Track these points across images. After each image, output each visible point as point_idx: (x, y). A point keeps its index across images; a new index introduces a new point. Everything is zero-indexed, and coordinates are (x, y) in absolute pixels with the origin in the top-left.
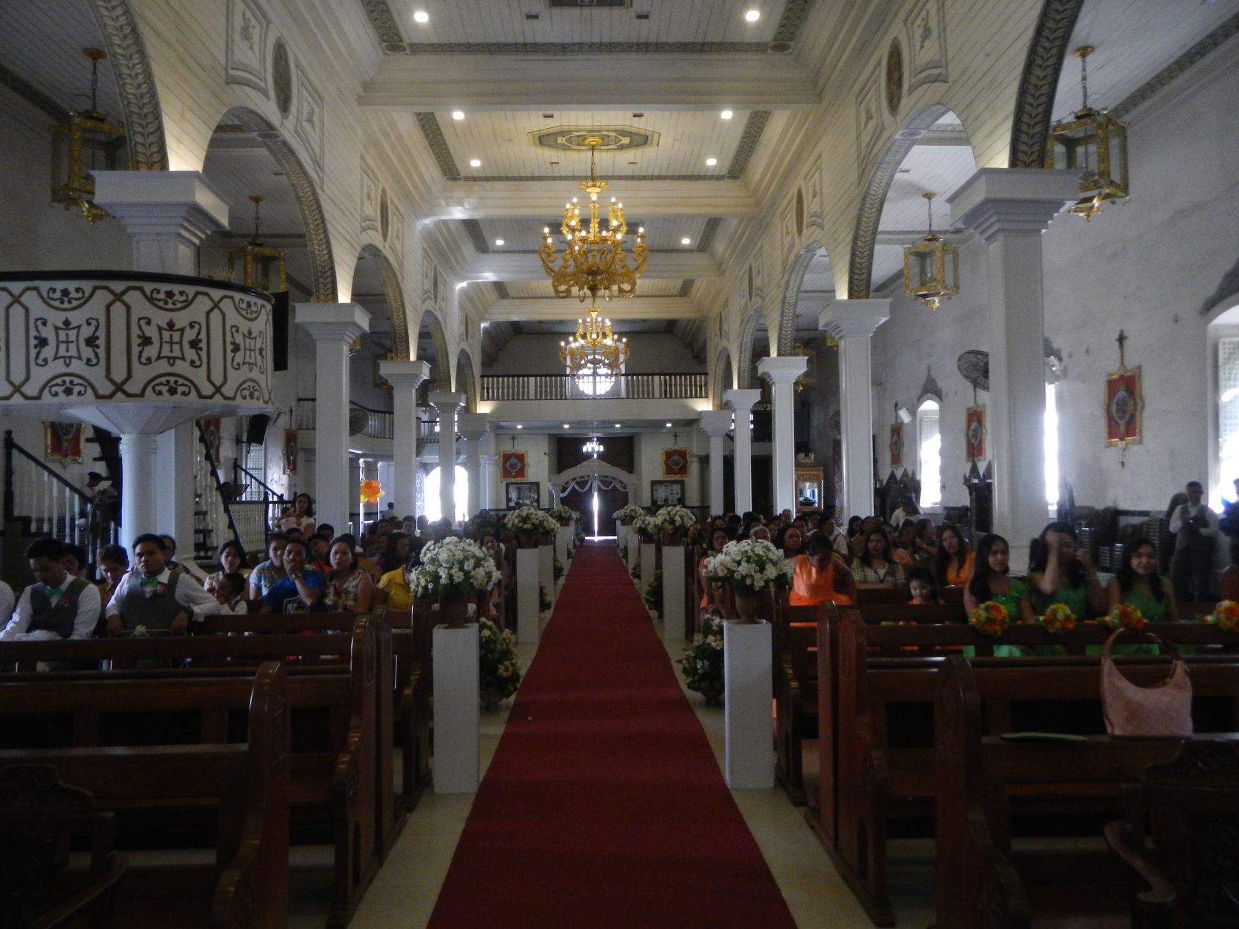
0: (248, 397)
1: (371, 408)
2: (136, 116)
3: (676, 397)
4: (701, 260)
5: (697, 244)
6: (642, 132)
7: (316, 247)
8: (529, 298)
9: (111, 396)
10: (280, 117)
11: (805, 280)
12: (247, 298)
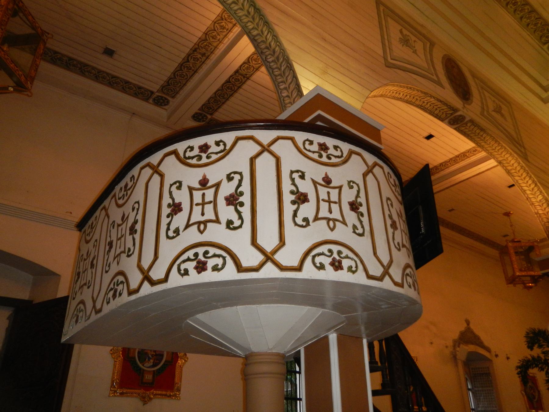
0: (329, 269)
10: (462, 103)
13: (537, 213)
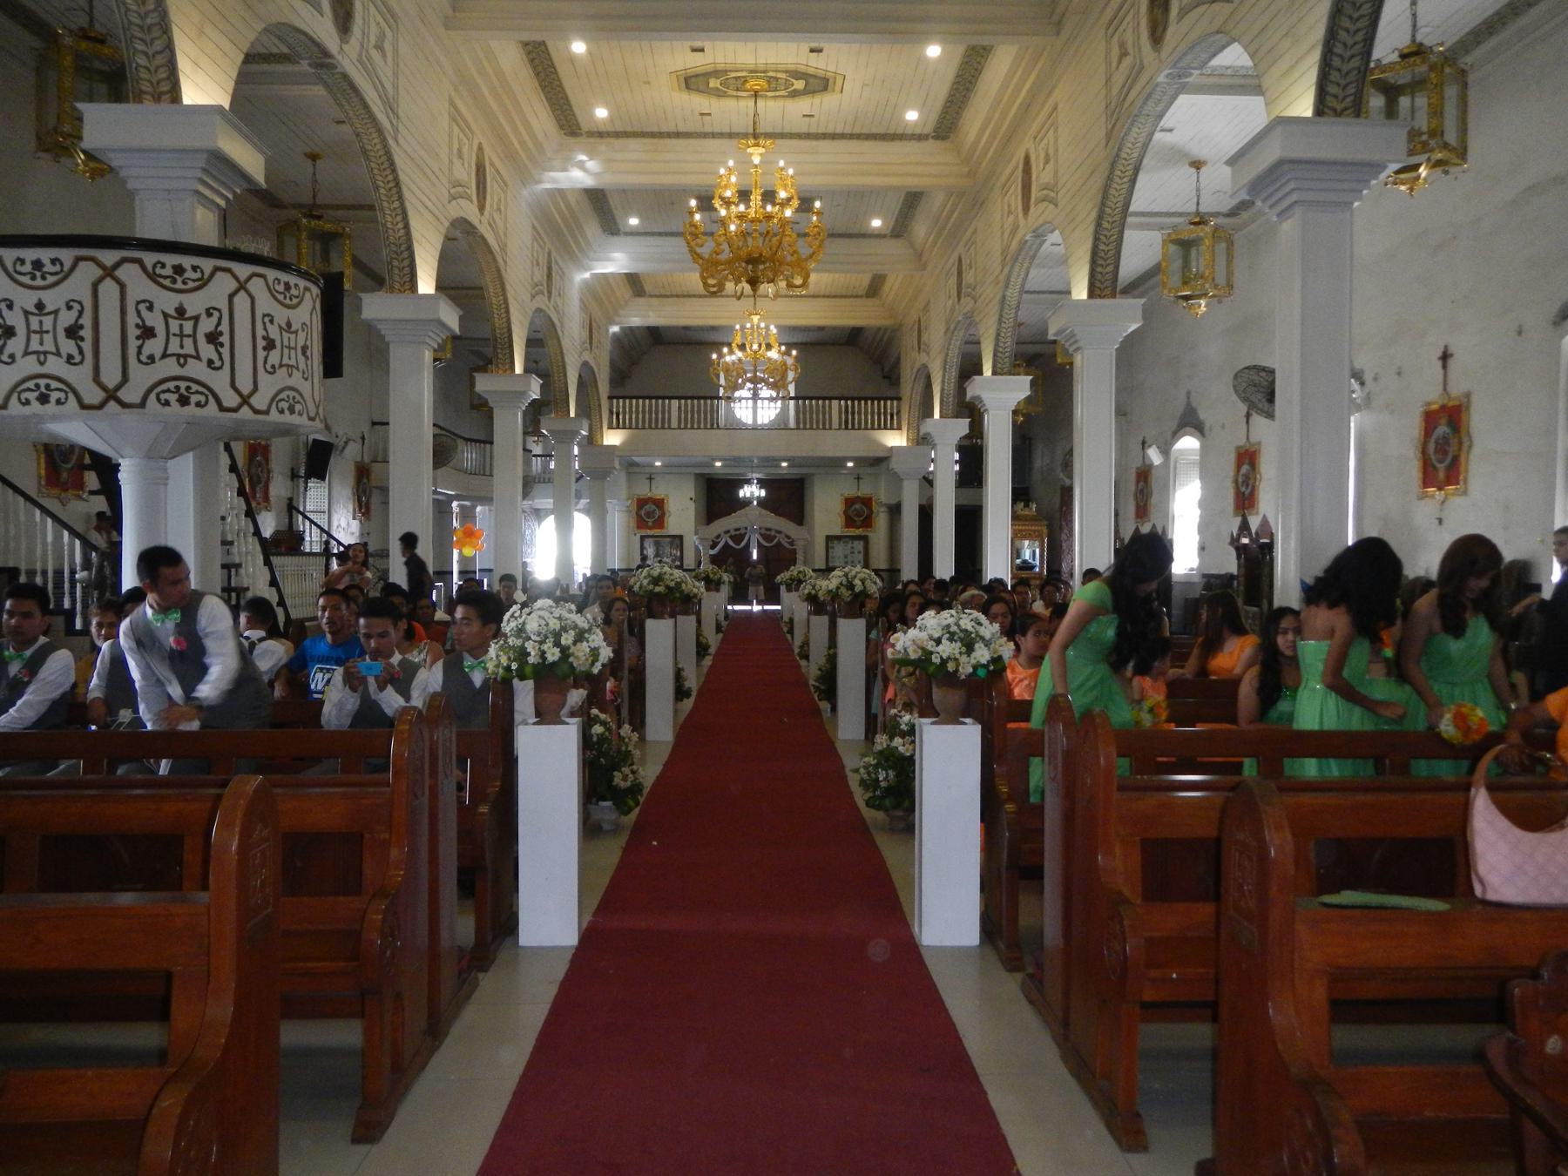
0: (287, 412)
1: (466, 436)
2: (136, 28)
3: (859, 429)
4: (895, 248)
5: (891, 227)
6: (821, 73)
7: (389, 218)
8: (672, 296)
9: (101, 406)
11: (1030, 276)
12: (284, 277)
13: (384, 225)
